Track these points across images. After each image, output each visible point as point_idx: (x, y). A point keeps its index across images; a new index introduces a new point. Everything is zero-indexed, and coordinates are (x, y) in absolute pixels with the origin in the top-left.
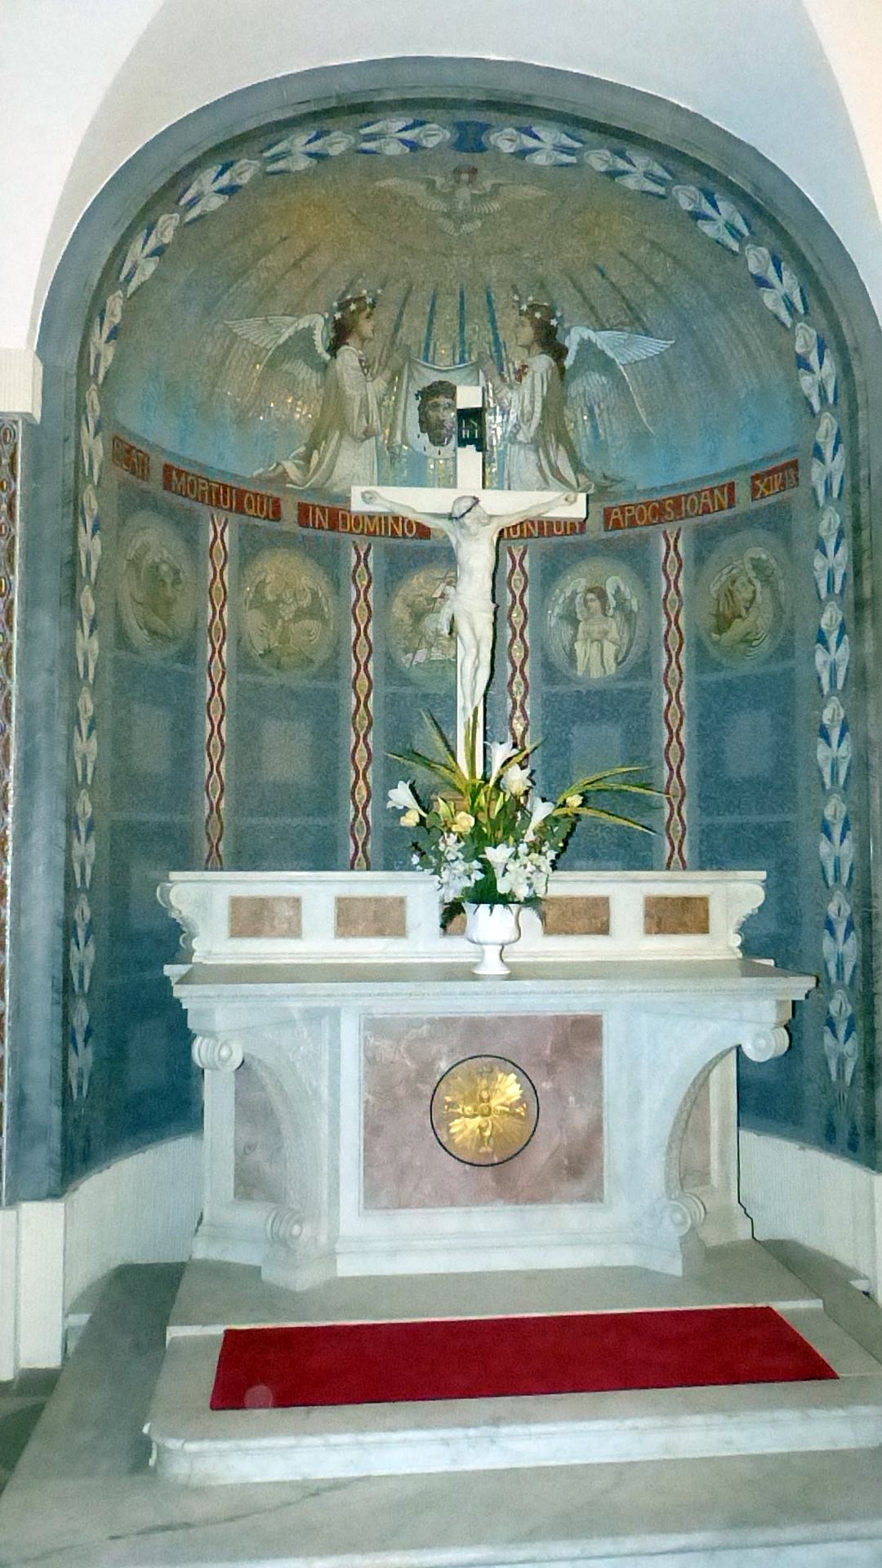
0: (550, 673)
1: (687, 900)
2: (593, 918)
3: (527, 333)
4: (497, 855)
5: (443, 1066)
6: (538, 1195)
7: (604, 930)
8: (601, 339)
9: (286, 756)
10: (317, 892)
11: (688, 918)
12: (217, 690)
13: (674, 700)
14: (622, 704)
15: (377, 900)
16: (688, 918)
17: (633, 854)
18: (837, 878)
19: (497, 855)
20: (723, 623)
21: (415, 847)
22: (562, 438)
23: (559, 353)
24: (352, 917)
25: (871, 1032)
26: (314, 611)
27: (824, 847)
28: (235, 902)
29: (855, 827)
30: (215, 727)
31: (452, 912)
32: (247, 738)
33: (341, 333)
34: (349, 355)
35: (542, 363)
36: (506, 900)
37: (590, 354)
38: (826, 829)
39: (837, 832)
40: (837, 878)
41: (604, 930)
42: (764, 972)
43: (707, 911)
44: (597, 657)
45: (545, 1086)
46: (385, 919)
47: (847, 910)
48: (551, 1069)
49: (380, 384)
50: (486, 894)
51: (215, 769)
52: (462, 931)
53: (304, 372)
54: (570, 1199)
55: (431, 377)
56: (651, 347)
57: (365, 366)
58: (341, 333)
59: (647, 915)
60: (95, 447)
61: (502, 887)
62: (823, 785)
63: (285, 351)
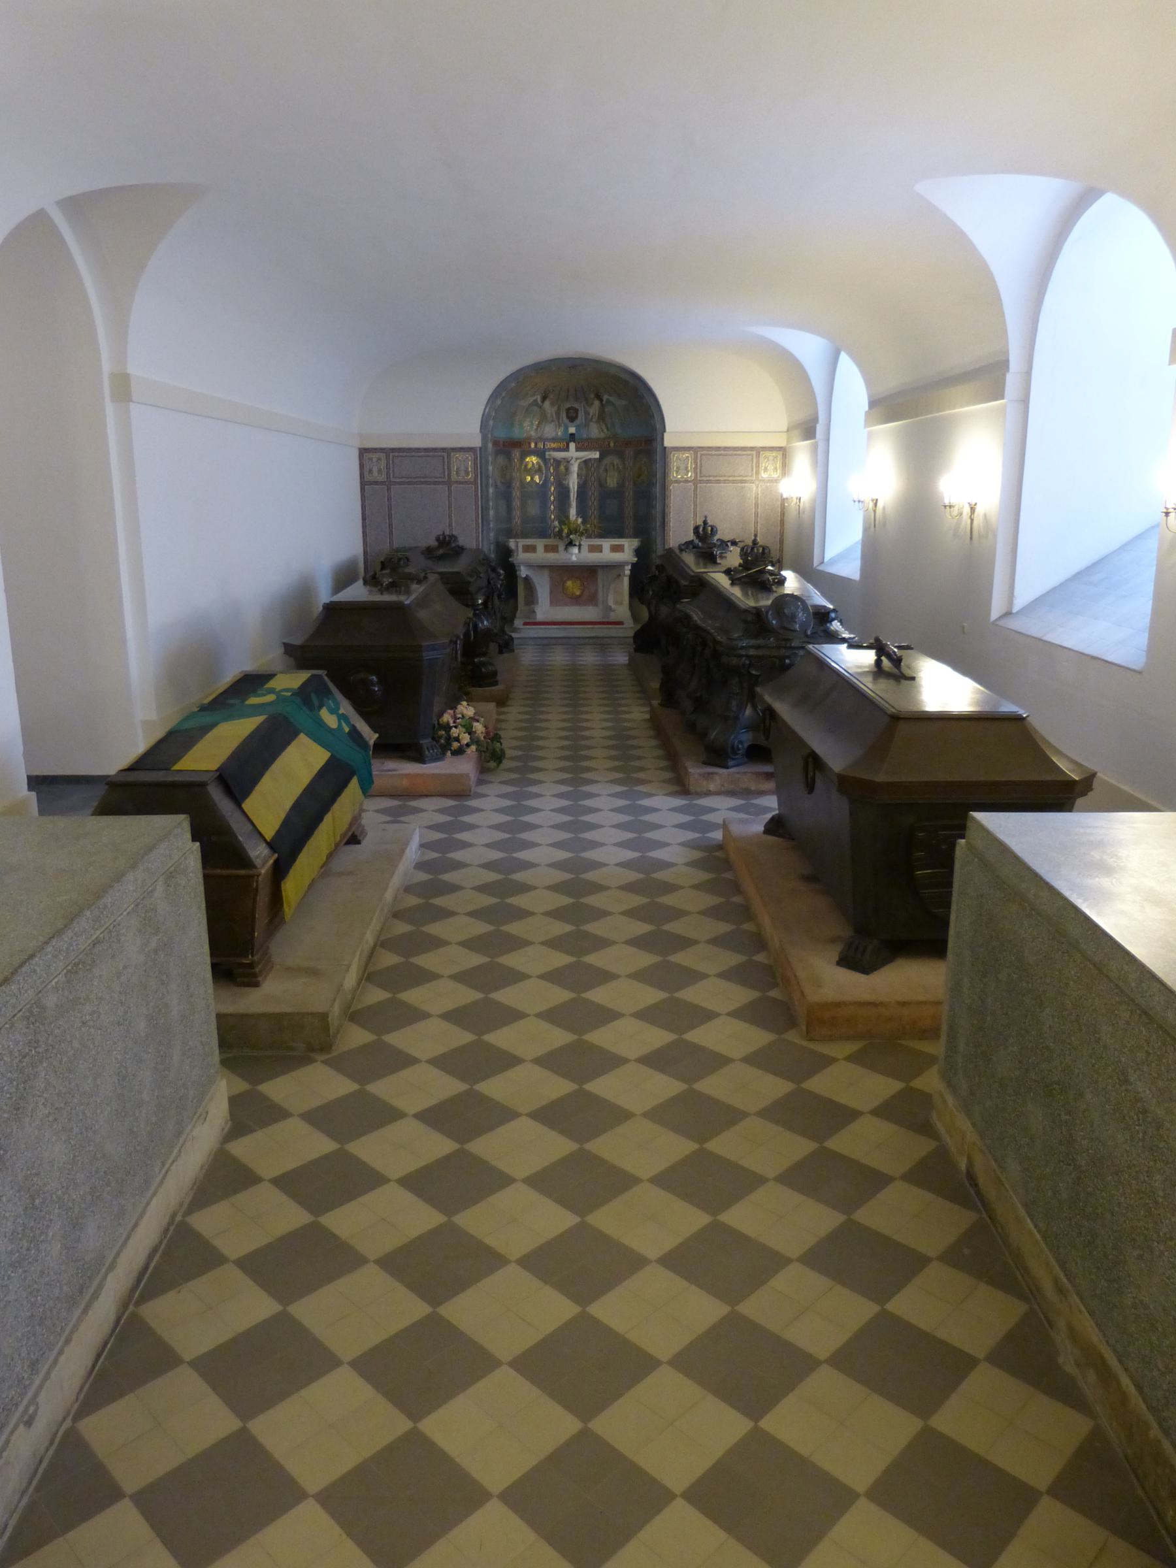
0: (601, 485)
2: (599, 549)
3: (592, 396)
6: (586, 604)
8: (611, 399)
9: (534, 510)
10: (540, 544)
12: (516, 493)
13: (629, 494)
14: (618, 493)
20: (639, 476)
21: (559, 534)
22: (603, 420)
23: (601, 400)
24: (548, 549)
26: (539, 470)
30: (517, 503)
31: (566, 549)
32: (524, 505)
33: (544, 399)
34: (547, 403)
35: (597, 403)
37: (608, 401)
44: (612, 482)
49: (556, 408)
50: (571, 544)
51: (517, 514)
53: (535, 408)
55: (568, 405)
56: (624, 403)
57: (552, 404)
58: (544, 399)
60: (490, 445)
63: (530, 405)
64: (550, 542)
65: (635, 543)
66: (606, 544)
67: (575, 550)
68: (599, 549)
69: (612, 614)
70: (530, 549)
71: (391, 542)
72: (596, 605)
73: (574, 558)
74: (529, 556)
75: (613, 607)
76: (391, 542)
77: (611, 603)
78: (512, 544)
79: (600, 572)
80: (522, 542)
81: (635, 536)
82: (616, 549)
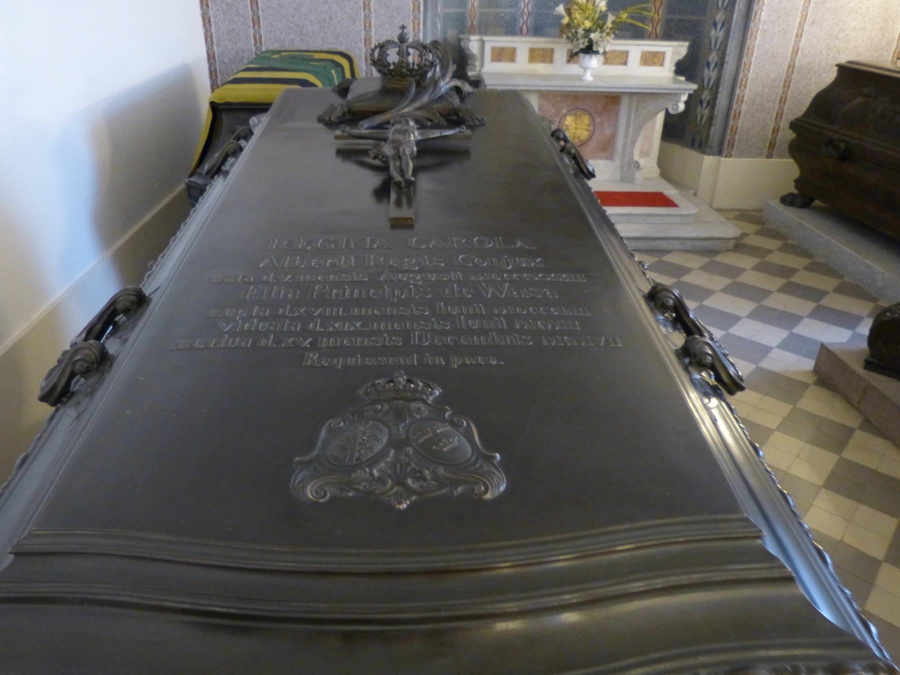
1: (657, 53)
2: (622, 58)
4: (592, 36)
5: (564, 111)
7: (625, 63)
10: (522, 45)
11: (656, 60)
15: (543, 49)
16: (656, 60)
17: (638, 34)
18: (715, 46)
19: (592, 36)
25: (714, 106)
27: (713, 33)
28: (493, 49)
29: (726, 26)
36: (597, 53)
38: (715, 25)
39: (719, 26)
40: (715, 46)
41: (625, 63)
42: (681, 82)
43: (664, 58)
45: (598, 120)
46: (546, 56)
47: (716, 59)
48: (601, 114)
50: (589, 50)
52: (577, 62)
54: (602, 158)
59: (642, 58)
61: (594, 49)
62: (718, 5)
64: (540, 42)
65: (674, 50)
66: (635, 49)
67: (594, 62)
68: (622, 58)
69: (638, 175)
70: (504, 55)
71: (258, 40)
72: (610, 158)
73: (589, 77)
74: (503, 67)
75: (642, 162)
76: (258, 40)
77: (636, 158)
78: (473, 44)
79: (625, 101)
80: (494, 42)
81: (667, 36)
82: (650, 59)
